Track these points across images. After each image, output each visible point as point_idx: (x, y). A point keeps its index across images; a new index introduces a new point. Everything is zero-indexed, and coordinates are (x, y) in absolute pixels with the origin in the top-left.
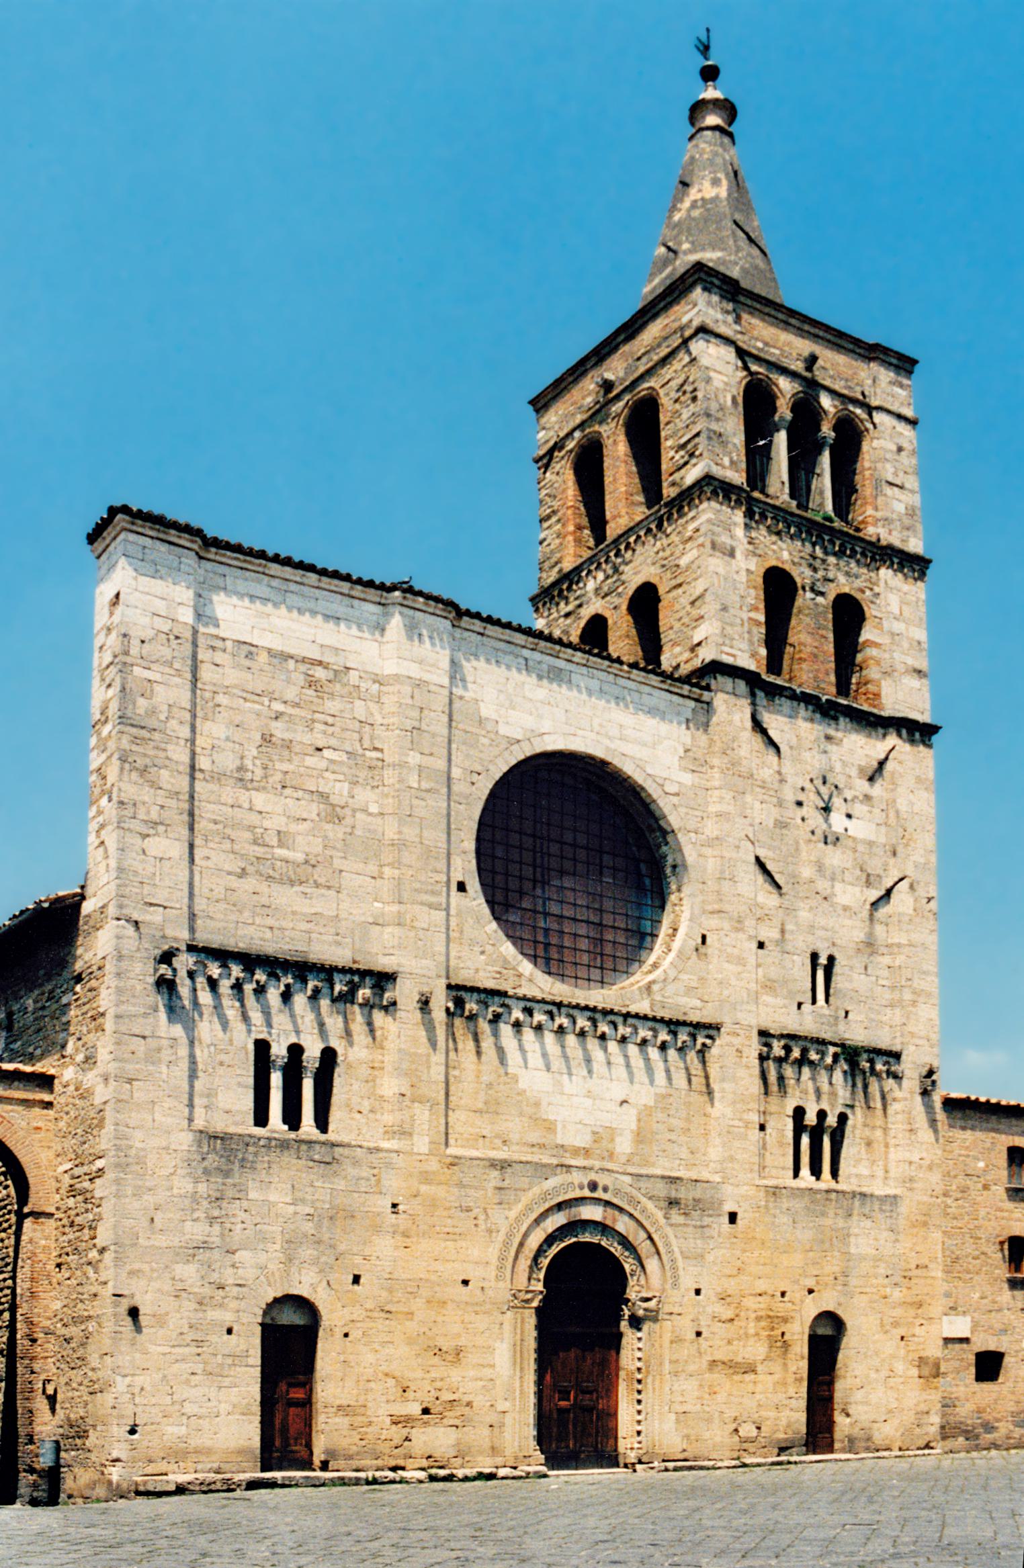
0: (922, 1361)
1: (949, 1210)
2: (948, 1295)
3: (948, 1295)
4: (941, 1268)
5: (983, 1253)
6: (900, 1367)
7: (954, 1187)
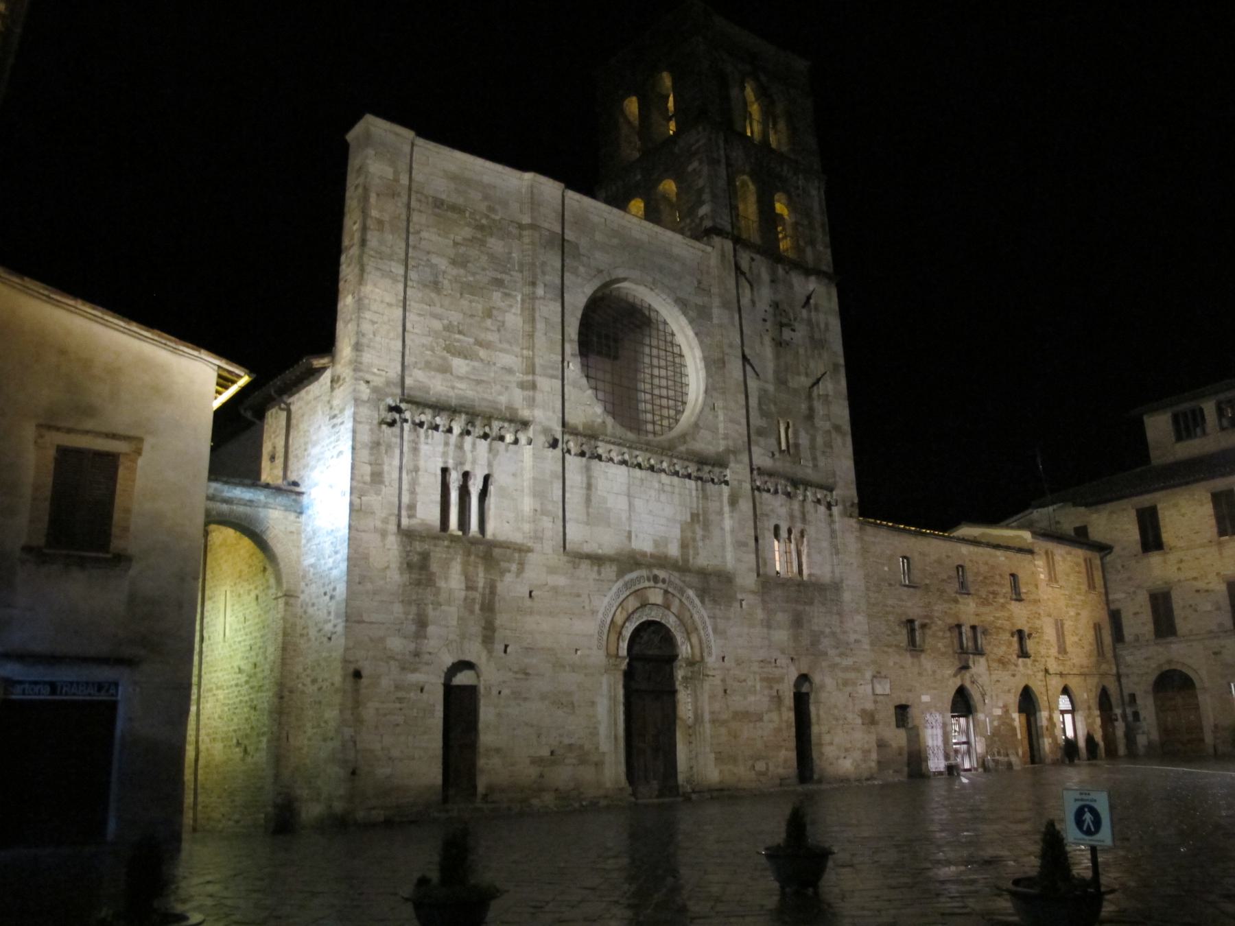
0: (864, 711)
2: (874, 662)
3: (874, 662)
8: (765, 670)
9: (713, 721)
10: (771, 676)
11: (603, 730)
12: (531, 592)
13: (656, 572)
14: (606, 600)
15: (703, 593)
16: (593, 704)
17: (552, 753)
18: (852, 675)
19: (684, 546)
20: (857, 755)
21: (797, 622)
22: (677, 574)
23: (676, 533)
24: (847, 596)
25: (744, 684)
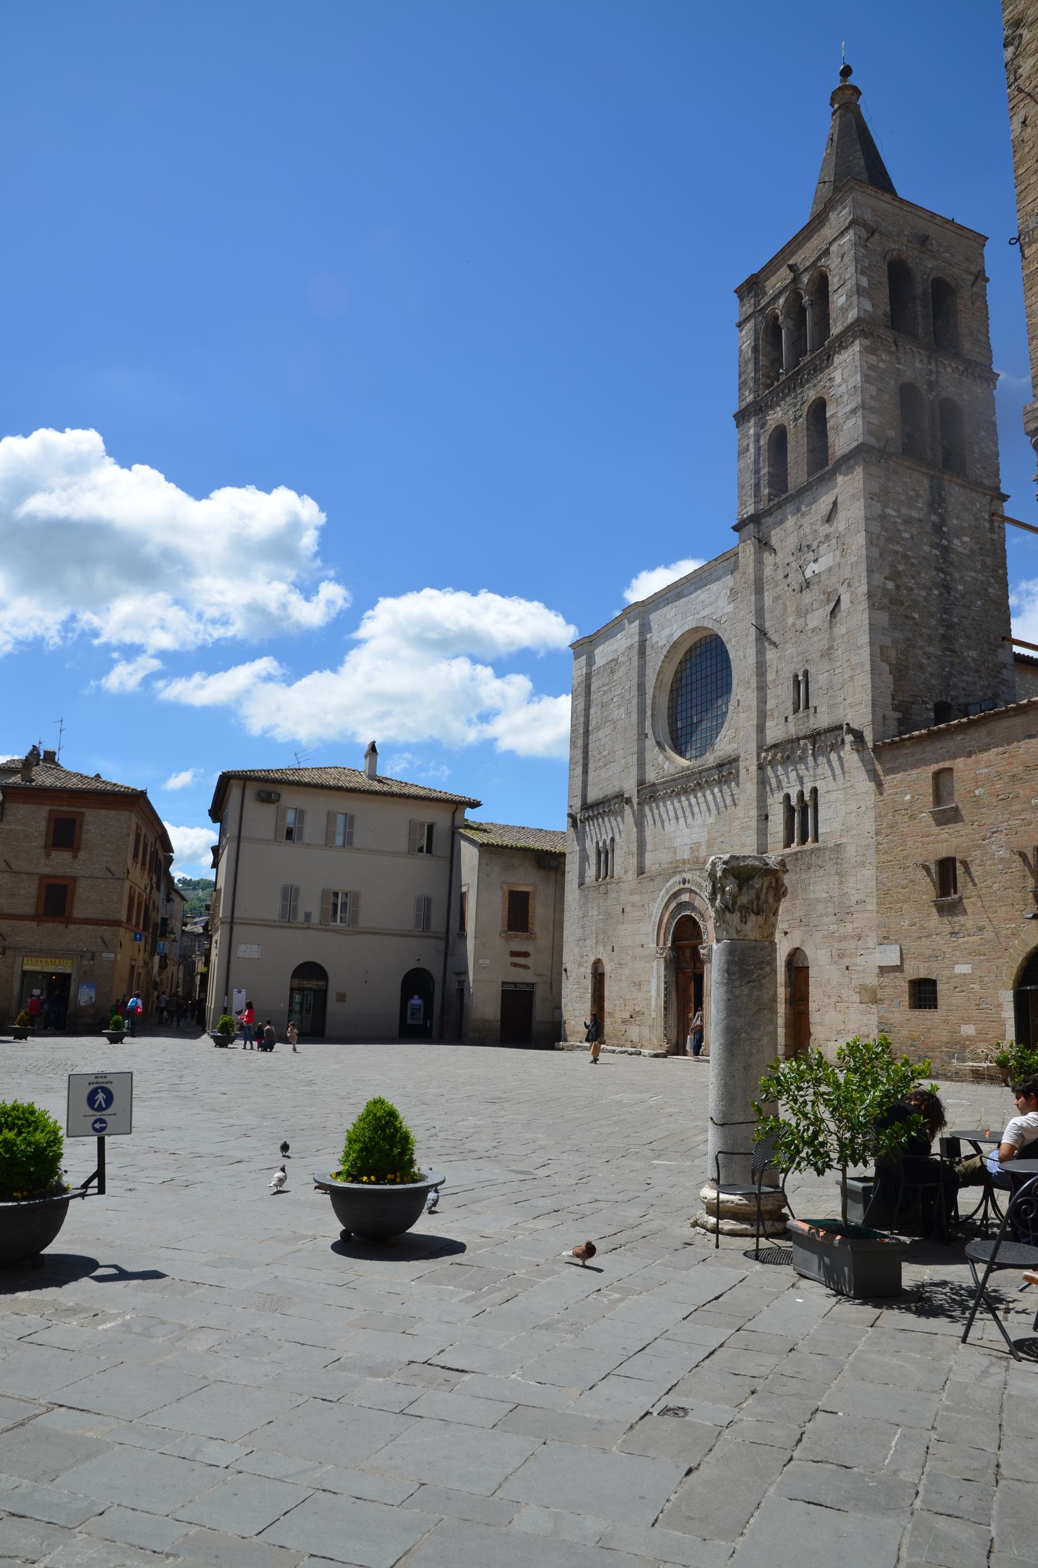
4: (875, 900)
6: (845, 993)
7: (884, 825)
11: (653, 1002)
13: (684, 875)
14: (657, 905)
16: (649, 982)
17: (631, 1017)
18: (851, 945)
19: (710, 844)
22: (697, 873)
23: (704, 837)
24: (850, 852)
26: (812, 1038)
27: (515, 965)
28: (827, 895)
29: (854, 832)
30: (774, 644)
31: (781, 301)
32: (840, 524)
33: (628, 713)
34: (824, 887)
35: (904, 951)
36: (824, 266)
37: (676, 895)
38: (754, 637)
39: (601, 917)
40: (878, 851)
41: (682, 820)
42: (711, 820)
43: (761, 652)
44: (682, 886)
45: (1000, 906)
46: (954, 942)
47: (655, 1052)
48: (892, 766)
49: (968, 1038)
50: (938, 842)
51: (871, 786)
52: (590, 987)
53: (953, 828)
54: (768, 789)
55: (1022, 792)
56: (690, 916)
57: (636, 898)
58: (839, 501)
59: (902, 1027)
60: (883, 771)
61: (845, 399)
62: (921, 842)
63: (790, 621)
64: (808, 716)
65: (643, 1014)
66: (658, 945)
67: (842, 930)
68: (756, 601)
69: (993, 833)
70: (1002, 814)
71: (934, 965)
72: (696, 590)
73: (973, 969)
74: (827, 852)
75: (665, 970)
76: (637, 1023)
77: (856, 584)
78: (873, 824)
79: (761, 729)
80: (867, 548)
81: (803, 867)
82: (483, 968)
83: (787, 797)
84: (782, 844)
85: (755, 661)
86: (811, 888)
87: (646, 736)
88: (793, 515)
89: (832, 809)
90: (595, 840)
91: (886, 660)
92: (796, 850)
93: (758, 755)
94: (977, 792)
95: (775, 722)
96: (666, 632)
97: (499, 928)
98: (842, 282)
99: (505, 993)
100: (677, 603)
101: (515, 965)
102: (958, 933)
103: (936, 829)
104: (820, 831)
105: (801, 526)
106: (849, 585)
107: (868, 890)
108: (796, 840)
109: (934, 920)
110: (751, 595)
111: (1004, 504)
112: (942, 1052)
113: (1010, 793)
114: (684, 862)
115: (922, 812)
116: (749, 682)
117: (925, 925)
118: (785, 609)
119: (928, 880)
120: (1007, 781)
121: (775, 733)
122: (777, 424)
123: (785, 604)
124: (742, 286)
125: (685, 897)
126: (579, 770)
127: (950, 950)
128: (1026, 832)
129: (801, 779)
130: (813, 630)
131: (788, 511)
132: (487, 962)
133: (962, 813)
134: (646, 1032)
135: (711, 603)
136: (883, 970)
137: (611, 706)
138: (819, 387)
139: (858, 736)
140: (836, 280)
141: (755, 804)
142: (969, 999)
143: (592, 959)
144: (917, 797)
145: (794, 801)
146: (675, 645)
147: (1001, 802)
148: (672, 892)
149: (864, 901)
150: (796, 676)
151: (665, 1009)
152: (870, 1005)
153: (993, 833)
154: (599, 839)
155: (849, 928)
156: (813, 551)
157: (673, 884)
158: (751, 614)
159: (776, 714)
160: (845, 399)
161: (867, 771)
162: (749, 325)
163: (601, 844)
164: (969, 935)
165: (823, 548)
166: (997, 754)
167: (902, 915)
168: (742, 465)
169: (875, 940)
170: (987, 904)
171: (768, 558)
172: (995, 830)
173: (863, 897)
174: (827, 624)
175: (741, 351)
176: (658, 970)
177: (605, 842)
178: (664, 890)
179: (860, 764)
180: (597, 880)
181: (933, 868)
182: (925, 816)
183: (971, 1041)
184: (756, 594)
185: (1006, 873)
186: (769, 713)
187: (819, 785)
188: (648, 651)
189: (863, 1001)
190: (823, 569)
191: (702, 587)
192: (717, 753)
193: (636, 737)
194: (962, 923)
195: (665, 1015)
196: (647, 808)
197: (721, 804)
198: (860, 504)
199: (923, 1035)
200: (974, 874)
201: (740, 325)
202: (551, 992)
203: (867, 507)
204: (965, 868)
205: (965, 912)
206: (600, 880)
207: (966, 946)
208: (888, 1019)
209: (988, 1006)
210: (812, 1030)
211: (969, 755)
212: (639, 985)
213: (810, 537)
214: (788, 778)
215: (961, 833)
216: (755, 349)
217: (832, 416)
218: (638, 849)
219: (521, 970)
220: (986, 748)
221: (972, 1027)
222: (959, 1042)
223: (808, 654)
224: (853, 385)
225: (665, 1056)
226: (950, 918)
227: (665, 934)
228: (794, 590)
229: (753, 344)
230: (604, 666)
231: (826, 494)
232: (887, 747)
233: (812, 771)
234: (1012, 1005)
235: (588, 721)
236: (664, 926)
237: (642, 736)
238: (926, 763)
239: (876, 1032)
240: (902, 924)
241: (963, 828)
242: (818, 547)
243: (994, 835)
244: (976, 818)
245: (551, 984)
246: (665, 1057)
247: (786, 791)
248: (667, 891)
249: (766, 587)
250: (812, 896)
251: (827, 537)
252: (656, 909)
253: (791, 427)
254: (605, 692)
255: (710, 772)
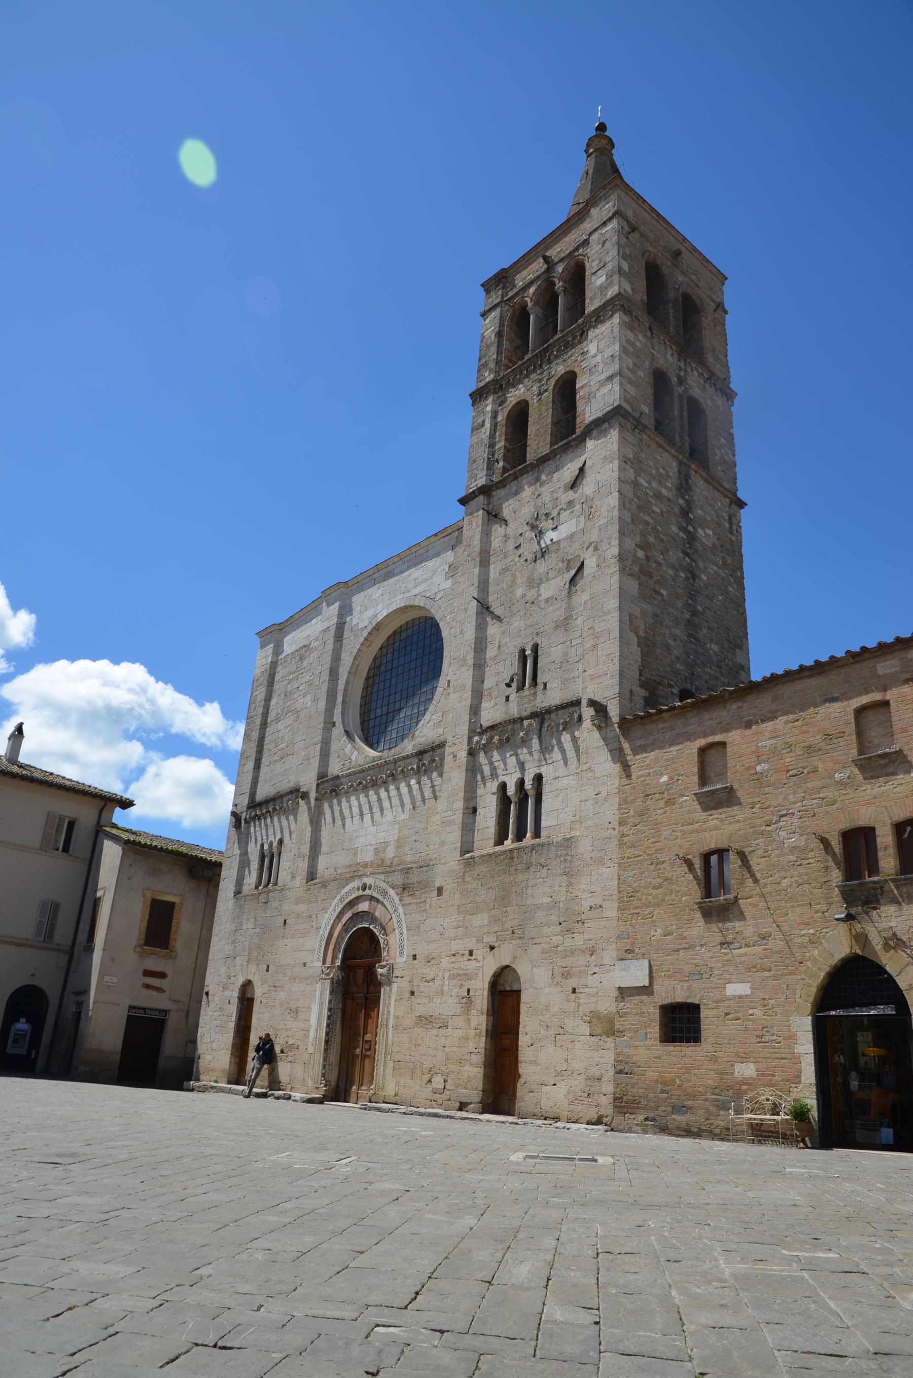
1: (625, 839)
4: (616, 905)
5: (666, 880)
6: (569, 1023)
7: (632, 813)
8: (456, 965)
9: (395, 1027)
10: (461, 972)
11: (312, 1033)
12: (285, 921)
13: (365, 880)
14: (327, 916)
15: (405, 888)
18: (580, 961)
19: (399, 844)
20: (578, 1083)
21: (504, 899)
22: (382, 877)
23: (393, 836)
24: (584, 847)
25: (431, 984)
26: (522, 1081)
27: (147, 986)
28: (550, 900)
29: (590, 823)
30: (499, 618)
31: (532, 290)
32: (587, 487)
33: (315, 700)
34: (547, 890)
35: (654, 968)
36: (582, 255)
37: (352, 904)
38: (474, 610)
39: (258, 930)
40: (621, 844)
41: (367, 818)
42: (406, 816)
43: (481, 628)
44: (361, 893)
45: (793, 907)
46: (725, 954)
47: (309, 1096)
48: (643, 743)
49: (745, 1081)
50: (705, 830)
51: (617, 768)
52: (234, 1014)
53: (726, 813)
54: (479, 777)
55: (820, 765)
56: (368, 929)
57: (302, 908)
58: (586, 467)
59: (649, 1067)
60: (632, 750)
61: (600, 369)
62: (681, 831)
63: (519, 592)
64: (535, 693)
65: (298, 1048)
66: (324, 963)
67: (569, 942)
68: (480, 573)
69: (781, 816)
70: (794, 793)
71: (696, 985)
72: (409, 568)
73: (752, 988)
74: (553, 849)
75: (331, 992)
76: (290, 1059)
77: (604, 546)
78: (617, 812)
79: (475, 710)
80: (620, 510)
81: (519, 867)
82: (109, 987)
83: (503, 787)
84: (492, 842)
85: (473, 636)
86: (529, 891)
87: (334, 724)
88: (530, 485)
89: (561, 798)
90: (259, 843)
91: (635, 631)
92: (510, 847)
93: (470, 739)
94: (759, 768)
95: (493, 702)
96: (370, 613)
97: (134, 942)
98: (602, 264)
99: (131, 1021)
100: (386, 583)
101: (147, 986)
102: (731, 943)
103: (704, 815)
104: (544, 824)
105: (539, 495)
106: (596, 549)
107: (606, 893)
108: (510, 836)
109: (698, 927)
110: (475, 567)
111: (741, 511)
112: (706, 1100)
113: (804, 768)
114: (366, 865)
115: (683, 795)
116: (464, 660)
117: (685, 934)
118: (514, 581)
119: (691, 877)
120: (801, 753)
121: (491, 714)
122: (518, 400)
123: (514, 575)
124: (491, 279)
125: (364, 906)
126: (250, 765)
127: (720, 965)
128: (827, 813)
129: (522, 766)
130: (547, 600)
131: (525, 481)
132: (115, 980)
133: (739, 794)
134: (299, 1071)
135: (425, 581)
136: (624, 993)
137: (296, 696)
138: (569, 362)
139: (600, 709)
140: (595, 264)
141: (462, 795)
142: (746, 1029)
143: (241, 980)
144: (676, 777)
145: (511, 791)
146: (378, 627)
147: (793, 779)
148: (347, 900)
149: (601, 906)
150: (523, 651)
151: (326, 1042)
152: (604, 1038)
153: (781, 816)
154: (265, 841)
155: (579, 940)
156: (553, 519)
157: (351, 890)
158: (472, 587)
159: (495, 693)
160: (600, 369)
161: (610, 751)
162: (495, 314)
163: (266, 847)
164: (748, 946)
165: (564, 515)
166: (786, 723)
167: (652, 922)
168: (476, 441)
169: (614, 955)
170: (772, 905)
171: (498, 531)
172: (785, 812)
173: (599, 901)
174: (565, 593)
175: (483, 337)
176: (322, 993)
177: (271, 844)
178: (338, 897)
179: (602, 743)
180: (257, 888)
181: (698, 863)
182: (689, 801)
183: (750, 1084)
184: (480, 566)
185: (801, 865)
186: (486, 693)
187: (544, 770)
188: (346, 634)
189: (595, 1033)
190: (564, 536)
191: (415, 565)
192: (418, 740)
193: (322, 725)
194: (737, 930)
195: (326, 1050)
196: (326, 806)
197: (418, 797)
198: (615, 465)
199: (679, 1077)
200: (755, 868)
201: (484, 315)
202: (187, 1022)
203: (621, 469)
204: (742, 861)
205: (742, 916)
206: (261, 888)
207: (743, 959)
208: (629, 1056)
209: (775, 1037)
210: (521, 1071)
211: (749, 725)
212: (295, 1012)
213: (550, 505)
214: (505, 764)
215: (737, 818)
216: (499, 334)
217: (583, 387)
218: (310, 851)
219: (155, 994)
220: (772, 717)
221: (752, 1066)
222: (732, 1087)
223: (540, 625)
224: (610, 354)
225: (320, 1101)
226: (720, 925)
227: (334, 950)
228: (526, 560)
229: (497, 329)
230: (292, 653)
231: (571, 461)
232: (639, 721)
233: (536, 755)
234: (810, 1036)
235: (267, 713)
236: (333, 940)
237: (329, 724)
238: (689, 737)
239: (612, 1072)
240: (652, 933)
241: (740, 813)
242: (559, 514)
243: (782, 819)
244: (758, 799)
245: (188, 1012)
246: (322, 1102)
247: (501, 779)
248: (342, 899)
249: (492, 559)
250: (529, 902)
251: (570, 503)
252: (326, 920)
253: (534, 402)
254: (290, 681)
255: (408, 761)
